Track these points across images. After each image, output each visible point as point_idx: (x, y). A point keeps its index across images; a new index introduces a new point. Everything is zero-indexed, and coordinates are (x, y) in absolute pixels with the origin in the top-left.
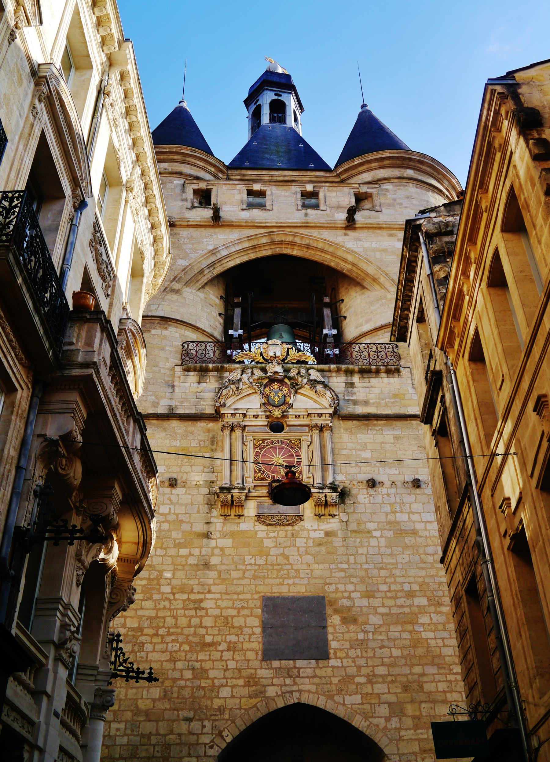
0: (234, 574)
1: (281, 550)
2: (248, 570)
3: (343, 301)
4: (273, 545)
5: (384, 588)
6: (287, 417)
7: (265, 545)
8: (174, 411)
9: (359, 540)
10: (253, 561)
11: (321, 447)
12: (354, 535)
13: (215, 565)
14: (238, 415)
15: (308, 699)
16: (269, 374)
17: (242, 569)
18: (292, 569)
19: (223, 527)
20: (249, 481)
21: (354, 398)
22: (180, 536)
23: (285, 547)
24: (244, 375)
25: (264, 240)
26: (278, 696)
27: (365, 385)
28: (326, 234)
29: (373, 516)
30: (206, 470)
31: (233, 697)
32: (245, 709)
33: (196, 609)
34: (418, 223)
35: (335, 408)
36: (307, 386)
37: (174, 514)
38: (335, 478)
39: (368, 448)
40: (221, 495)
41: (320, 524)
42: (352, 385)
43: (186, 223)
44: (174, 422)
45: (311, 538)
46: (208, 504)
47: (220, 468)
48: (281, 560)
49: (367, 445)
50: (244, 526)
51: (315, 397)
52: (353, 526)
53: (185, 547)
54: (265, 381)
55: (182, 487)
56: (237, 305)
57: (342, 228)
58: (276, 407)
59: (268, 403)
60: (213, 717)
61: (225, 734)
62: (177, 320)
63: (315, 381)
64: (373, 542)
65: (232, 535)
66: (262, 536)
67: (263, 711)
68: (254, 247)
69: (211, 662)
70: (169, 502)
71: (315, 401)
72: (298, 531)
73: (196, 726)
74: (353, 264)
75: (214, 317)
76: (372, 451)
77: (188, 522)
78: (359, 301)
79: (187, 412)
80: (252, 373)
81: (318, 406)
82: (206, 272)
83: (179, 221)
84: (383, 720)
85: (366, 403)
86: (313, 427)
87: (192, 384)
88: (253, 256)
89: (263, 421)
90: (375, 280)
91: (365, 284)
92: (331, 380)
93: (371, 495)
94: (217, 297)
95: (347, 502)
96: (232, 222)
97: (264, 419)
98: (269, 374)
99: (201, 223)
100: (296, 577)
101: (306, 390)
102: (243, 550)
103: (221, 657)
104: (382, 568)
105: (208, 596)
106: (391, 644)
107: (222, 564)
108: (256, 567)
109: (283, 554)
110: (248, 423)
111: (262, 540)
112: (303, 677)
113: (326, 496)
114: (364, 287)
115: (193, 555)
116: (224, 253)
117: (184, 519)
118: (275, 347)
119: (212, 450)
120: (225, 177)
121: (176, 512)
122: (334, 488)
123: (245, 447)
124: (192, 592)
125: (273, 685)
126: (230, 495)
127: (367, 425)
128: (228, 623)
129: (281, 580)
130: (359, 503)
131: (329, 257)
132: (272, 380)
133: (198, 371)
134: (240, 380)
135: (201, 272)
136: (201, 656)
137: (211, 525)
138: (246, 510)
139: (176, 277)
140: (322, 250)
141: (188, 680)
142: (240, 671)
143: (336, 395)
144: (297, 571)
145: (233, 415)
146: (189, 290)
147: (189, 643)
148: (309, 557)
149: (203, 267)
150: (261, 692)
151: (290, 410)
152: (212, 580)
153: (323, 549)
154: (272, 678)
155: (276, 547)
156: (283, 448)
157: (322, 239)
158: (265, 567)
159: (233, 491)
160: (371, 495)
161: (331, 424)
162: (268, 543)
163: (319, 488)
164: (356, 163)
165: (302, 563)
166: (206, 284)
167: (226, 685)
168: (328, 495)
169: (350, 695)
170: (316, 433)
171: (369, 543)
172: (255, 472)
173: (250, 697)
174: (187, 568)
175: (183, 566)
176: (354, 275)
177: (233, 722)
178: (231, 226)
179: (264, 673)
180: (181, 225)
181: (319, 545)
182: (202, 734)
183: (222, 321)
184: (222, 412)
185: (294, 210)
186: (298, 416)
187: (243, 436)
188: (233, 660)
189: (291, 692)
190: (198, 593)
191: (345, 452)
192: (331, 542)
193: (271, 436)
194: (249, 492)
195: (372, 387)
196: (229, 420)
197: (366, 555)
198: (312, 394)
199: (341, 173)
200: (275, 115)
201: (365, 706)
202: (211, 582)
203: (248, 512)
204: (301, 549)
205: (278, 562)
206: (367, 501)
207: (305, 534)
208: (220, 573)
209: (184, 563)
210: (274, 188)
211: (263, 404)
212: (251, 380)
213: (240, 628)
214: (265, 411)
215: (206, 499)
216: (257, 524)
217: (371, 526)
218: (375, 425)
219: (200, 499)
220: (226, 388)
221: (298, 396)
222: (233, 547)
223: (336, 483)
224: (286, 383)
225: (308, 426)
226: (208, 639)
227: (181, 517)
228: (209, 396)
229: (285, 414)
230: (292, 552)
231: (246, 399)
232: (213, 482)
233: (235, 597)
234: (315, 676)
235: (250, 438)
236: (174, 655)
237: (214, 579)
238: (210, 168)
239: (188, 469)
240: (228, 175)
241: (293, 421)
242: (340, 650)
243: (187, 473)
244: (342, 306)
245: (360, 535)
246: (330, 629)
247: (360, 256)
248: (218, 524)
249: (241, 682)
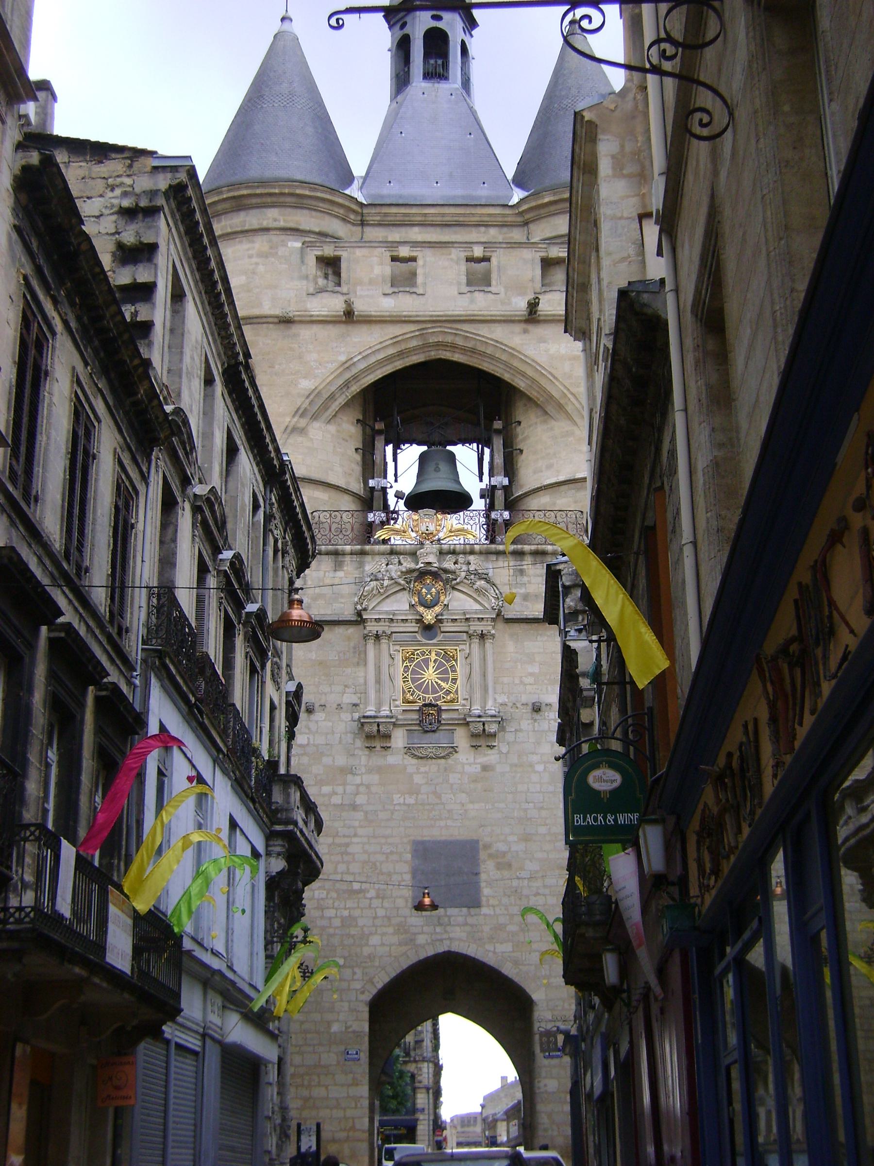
0: (382, 815)
3: (519, 423)
4: (424, 781)
5: (542, 830)
6: (440, 621)
7: (415, 782)
9: (519, 775)
13: (361, 805)
15: (459, 947)
22: (322, 772)
23: (437, 784)
25: (414, 343)
26: (428, 944)
28: (498, 333)
30: (347, 690)
31: (383, 945)
32: (395, 957)
33: (342, 854)
34: (558, 567)
35: (499, 610)
37: (314, 745)
39: (537, 659)
42: (522, 572)
43: (308, 319)
46: (351, 732)
52: (514, 759)
56: (380, 432)
57: (520, 321)
58: (428, 606)
60: (363, 965)
61: (376, 980)
64: (535, 778)
65: (379, 770)
67: (413, 958)
68: (401, 354)
69: (359, 910)
70: (307, 731)
71: (475, 599)
73: (348, 972)
74: (533, 380)
81: (478, 607)
83: (299, 316)
84: (533, 968)
88: (399, 365)
89: (413, 627)
90: (560, 407)
91: (549, 409)
94: (353, 423)
96: (371, 316)
97: (414, 624)
99: (329, 319)
100: (448, 818)
103: (370, 904)
104: (542, 808)
105: (355, 840)
106: (547, 891)
108: (405, 808)
109: (435, 793)
112: (453, 925)
114: (546, 413)
115: (337, 794)
116: (362, 366)
120: (359, 218)
121: (316, 743)
124: (337, 835)
125: (423, 933)
128: (376, 869)
129: (433, 822)
131: (501, 366)
135: (332, 397)
136: (349, 904)
138: (393, 740)
140: (492, 357)
141: (337, 927)
142: (389, 918)
144: (450, 811)
146: (316, 424)
147: (337, 891)
148: (464, 795)
149: (333, 389)
150: (411, 940)
154: (422, 926)
155: (427, 783)
157: (492, 340)
161: (493, 632)
162: (418, 779)
164: (546, 200)
165: (455, 803)
167: (376, 933)
169: (501, 943)
172: (404, 692)
173: (400, 944)
176: (533, 394)
177: (383, 969)
178: (369, 321)
179: (417, 920)
180: (301, 322)
181: (475, 781)
182: (353, 980)
183: (358, 458)
185: (456, 292)
188: (382, 907)
189: (441, 940)
190: (344, 836)
196: (372, 628)
199: (523, 212)
200: (432, 62)
201: (515, 954)
202: (357, 824)
204: (455, 786)
208: (366, 813)
210: (428, 252)
213: (389, 874)
216: (406, 756)
217: (535, 758)
221: (456, 593)
225: (467, 632)
226: (356, 886)
231: (392, 598)
232: (355, 705)
233: (383, 841)
234: (466, 924)
235: (398, 647)
236: (322, 902)
238: (337, 210)
239: (326, 689)
240: (362, 215)
242: (493, 897)
246: (483, 876)
247: (544, 368)
249: (391, 930)
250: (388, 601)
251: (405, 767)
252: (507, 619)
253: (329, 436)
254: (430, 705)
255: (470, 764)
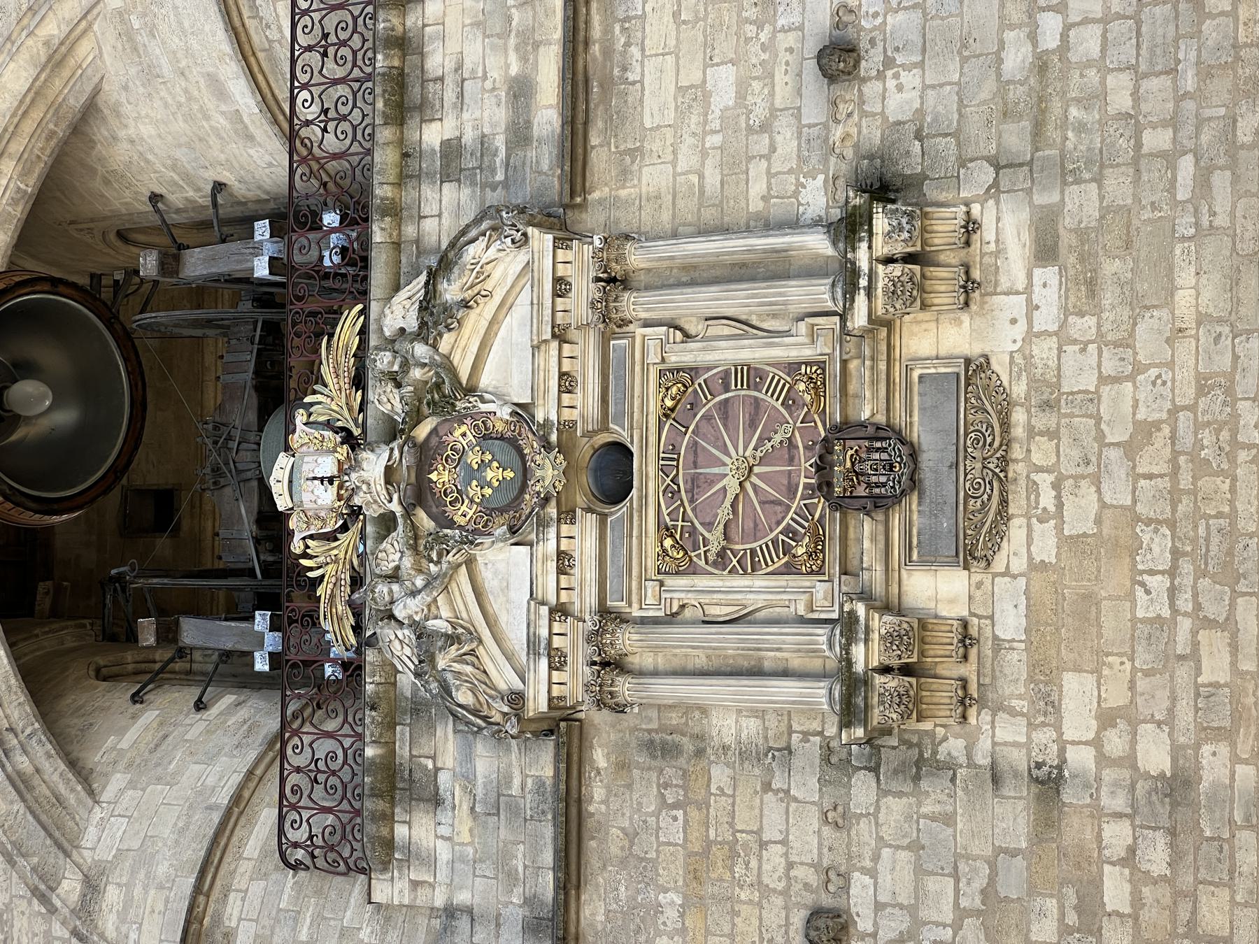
0: (1215, 668)
1: (1113, 454)
2: (1198, 606)
3: (155, 198)
8: (546, 912)
9: (1074, 112)
10: (1158, 583)
11: (693, 283)
12: (1052, 132)
13: (1176, 752)
14: (557, 642)
16: (395, 507)
17: (1194, 633)
18: (1192, 408)
19: (1013, 713)
20: (822, 594)
21: (500, 142)
22: (1051, 904)
23: (1100, 436)
24: (399, 612)
27: (450, 95)
29: (976, 48)
36: (444, 346)
38: (816, 223)
39: (696, 77)
40: (876, 717)
41: (1004, 284)
42: (452, 150)
44: (586, 912)
45: (1063, 325)
46: (917, 778)
47: (772, 722)
48: (1154, 459)
49: (684, 83)
50: (1010, 622)
51: (487, 309)
53: (1097, 884)
54: (425, 522)
55: (846, 888)
56: (168, 634)
58: (525, 473)
59: (514, 515)
62: (197, 889)
63: (426, 306)
66: (1052, 541)
71: (505, 306)
72: (1032, 380)
75: (208, 732)
76: (709, 63)
77: (993, 865)
78: (146, 130)
79: (548, 857)
80: (394, 576)
82: (23, 762)
85: (521, 91)
86: (605, 319)
87: (443, 830)
90: (57, 59)
91: (76, 103)
92: (430, 240)
93: (889, 63)
95: (912, 165)
97: (575, 530)
98: (395, 507)
100: (1229, 391)
101: (460, 347)
102: (1112, 624)
107: (1168, 722)
108: (1186, 567)
109: (1130, 449)
110: (591, 599)
111: (1071, 543)
113: (888, 260)
114: (90, 110)
117: (980, 882)
118: (305, 476)
119: (700, 753)
122: (850, 227)
123: (688, 613)
126: (879, 679)
127: (608, 84)
130: (920, 112)
132: (421, 494)
133: (393, 806)
134: (421, 633)
137: (1003, 765)
139: (35, 891)
143: (477, 221)
144: (1203, 389)
145: (557, 661)
146: (89, 839)
151: (540, 417)
152: (1240, 769)
153: (1110, 267)
156: (694, 446)
158: (1184, 528)
159: (859, 667)
160: (889, 63)
163: (851, 289)
166: (73, 764)
168: (881, 248)
170: (632, 304)
171: (1089, 64)
172: (789, 569)
174: (1186, 880)
175: (1178, 895)
181: (1092, 286)
184: (543, 706)
186: (567, 383)
187: (643, 621)
191: (713, 178)
192: (1081, 233)
193: (643, 498)
194: (865, 596)
195: (459, 67)
196: (575, 681)
197: (1139, 77)
198: (475, 322)
203: (952, 601)
204: (1109, 368)
205: (1164, 468)
206: (911, 79)
207: (1044, 351)
209: (1164, 892)
211: (513, 531)
212: (419, 582)
214: (543, 524)
215: (895, 786)
216: (999, 564)
217: (1016, 58)
218: (608, 52)
219: (895, 807)
220: (446, 689)
221: (486, 380)
222: (1097, 671)
223: (836, 214)
224: (434, 431)
227: (971, 900)
228: (485, 762)
229: (554, 438)
230: (1122, 407)
231: (496, 605)
237: (1236, 759)
241: (586, 402)
243: (790, 865)
244: (175, 199)
245: (1056, 106)
248: (1001, 735)
250: (503, 619)
251: (1037, 567)
252: (573, 194)
253: (130, 792)
254: (823, 467)
255: (1032, 307)
